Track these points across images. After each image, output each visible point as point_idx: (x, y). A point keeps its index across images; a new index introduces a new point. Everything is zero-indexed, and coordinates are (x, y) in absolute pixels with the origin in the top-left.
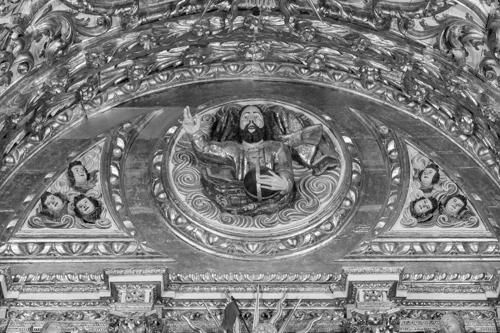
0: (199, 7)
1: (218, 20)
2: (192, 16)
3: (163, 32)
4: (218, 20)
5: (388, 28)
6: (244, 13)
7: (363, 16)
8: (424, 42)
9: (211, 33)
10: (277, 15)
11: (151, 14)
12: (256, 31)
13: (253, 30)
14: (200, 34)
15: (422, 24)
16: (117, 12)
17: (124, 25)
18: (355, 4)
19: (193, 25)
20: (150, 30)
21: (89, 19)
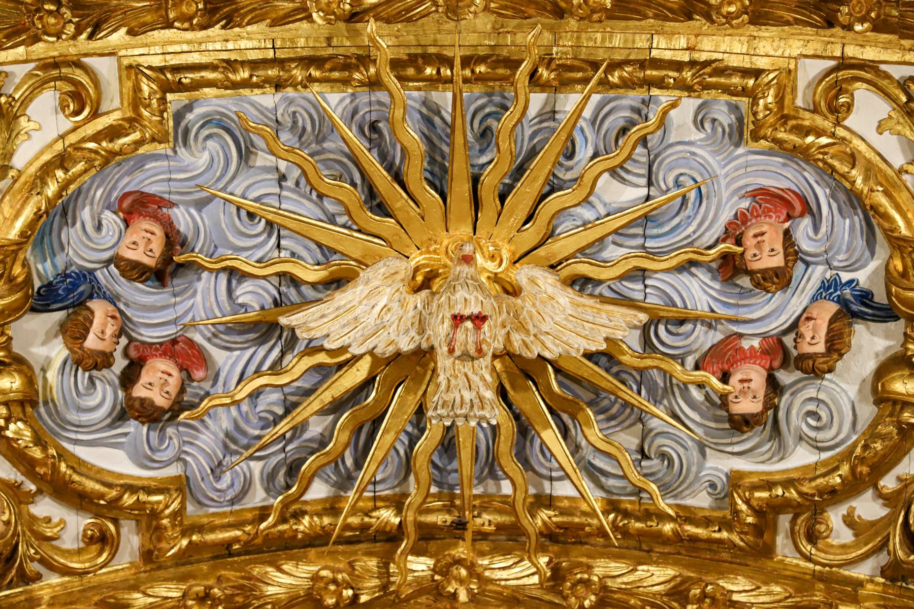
0: (326, 521)
1: (372, 563)
2: (312, 552)
3: (241, 587)
4: (372, 563)
5: (768, 551)
6: (433, 546)
7: (707, 522)
8: (861, 572)
9: (356, 597)
10: (506, 552)
11: (213, 529)
12: (463, 597)
13: (454, 596)
14: (330, 601)
15: (849, 521)
16: (128, 500)
17: (148, 555)
18: (689, 502)
19: (315, 578)
20: (211, 582)
21: (62, 521)
